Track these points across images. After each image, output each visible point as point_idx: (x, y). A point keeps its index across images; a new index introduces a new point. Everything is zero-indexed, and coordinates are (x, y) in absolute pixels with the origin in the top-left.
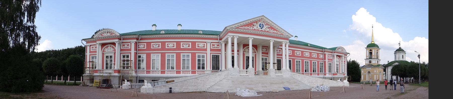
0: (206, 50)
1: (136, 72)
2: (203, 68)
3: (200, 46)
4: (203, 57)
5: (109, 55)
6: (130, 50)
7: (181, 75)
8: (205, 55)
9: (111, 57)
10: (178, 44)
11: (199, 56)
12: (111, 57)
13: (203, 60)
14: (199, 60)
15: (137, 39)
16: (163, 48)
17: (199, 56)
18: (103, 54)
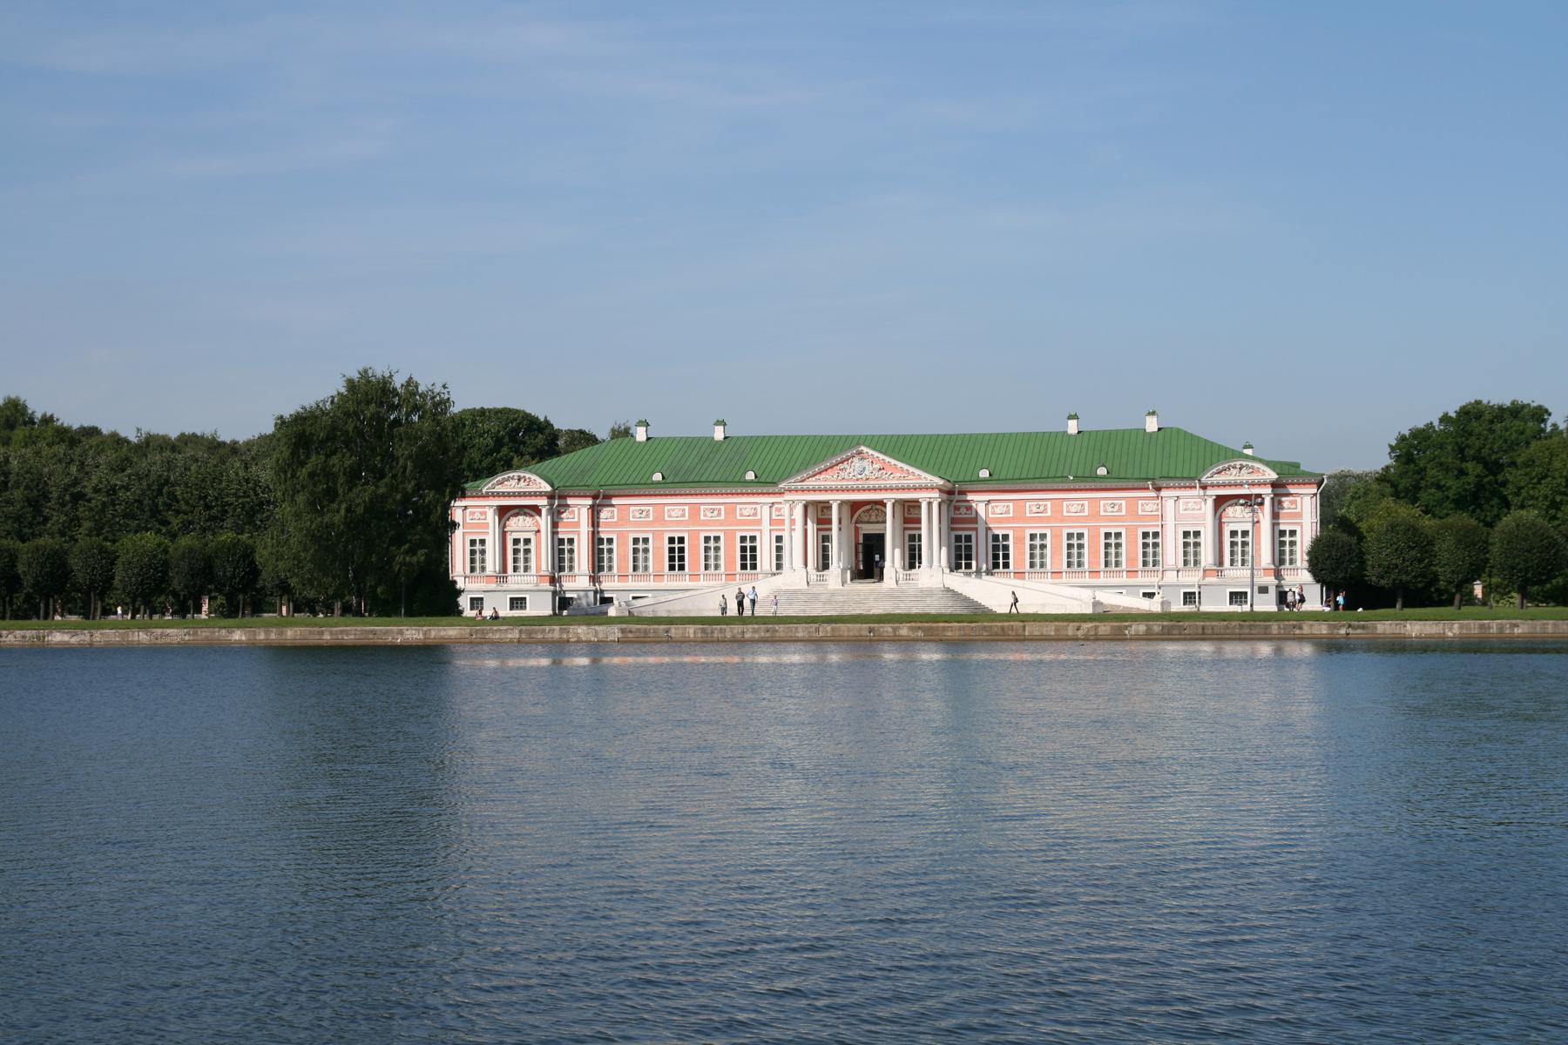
0: (759, 522)
1: (594, 579)
2: (754, 567)
3: (745, 513)
4: (753, 539)
5: (522, 536)
6: (578, 524)
7: (702, 583)
9: (527, 541)
10: (695, 510)
11: (743, 539)
12: (527, 541)
13: (753, 549)
14: (743, 549)
15: (595, 497)
16: (659, 519)
17: (743, 539)
18: (504, 535)
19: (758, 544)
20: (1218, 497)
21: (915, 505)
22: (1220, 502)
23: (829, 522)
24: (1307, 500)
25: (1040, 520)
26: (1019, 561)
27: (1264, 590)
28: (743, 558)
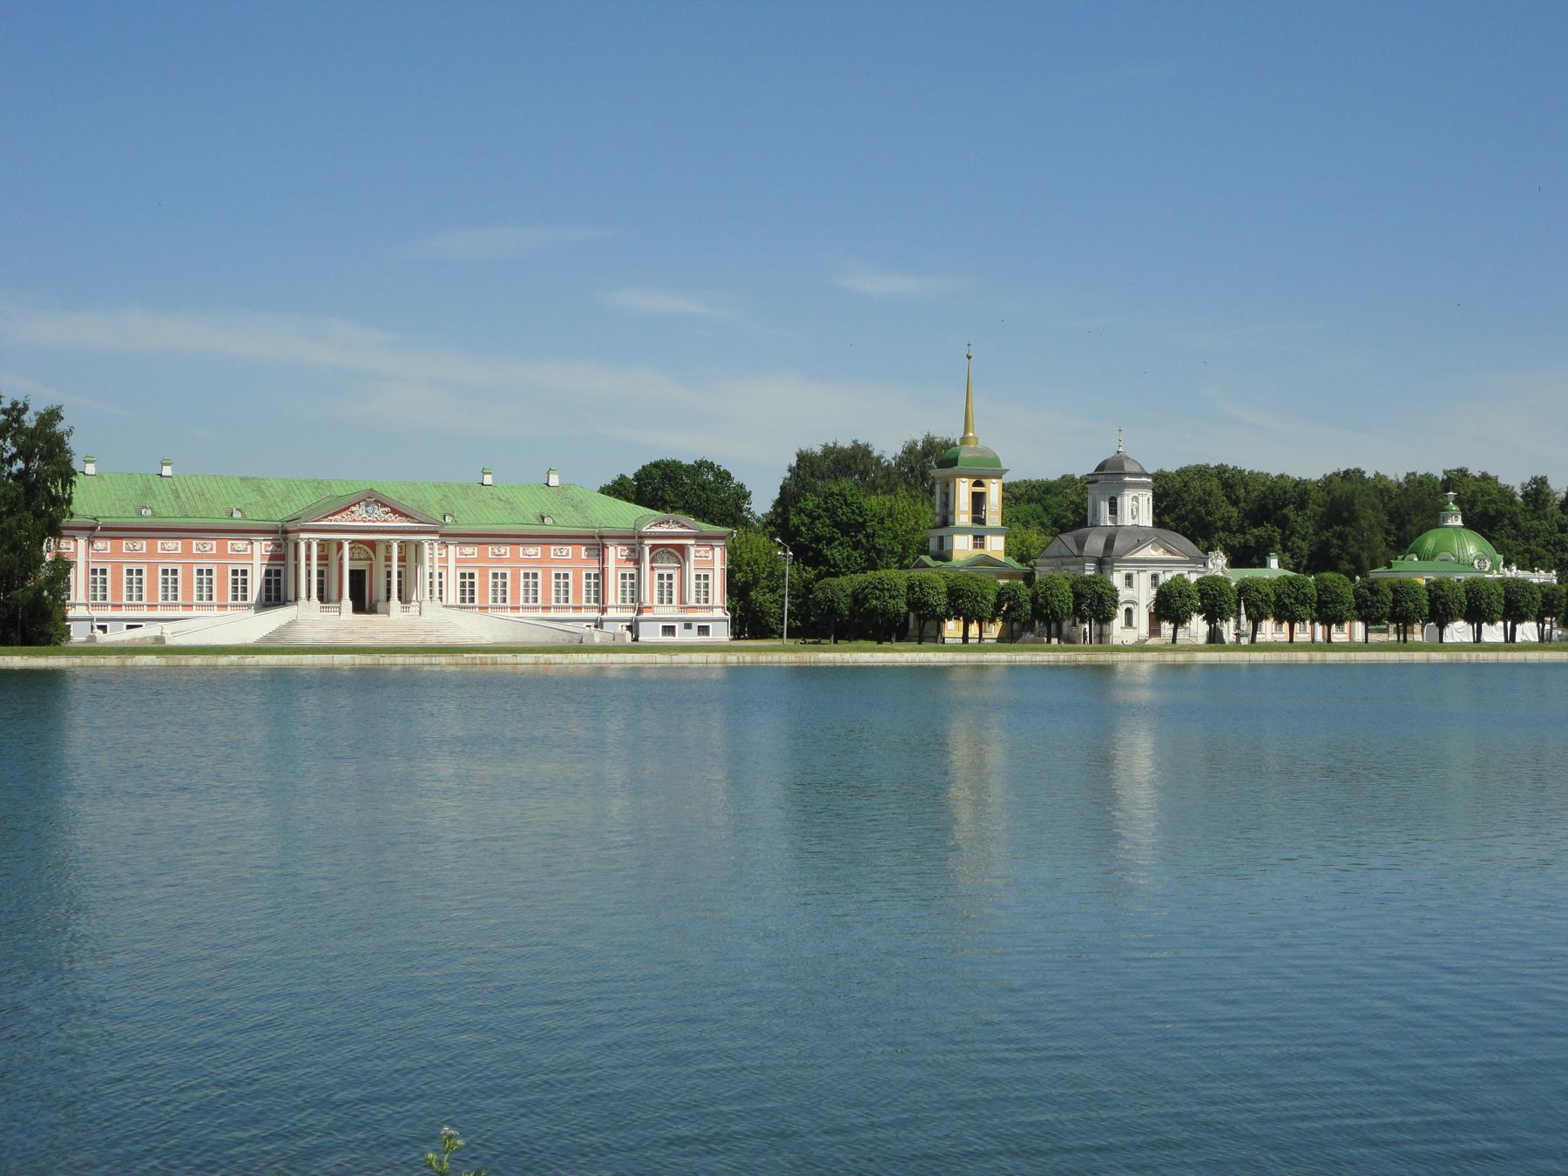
0: (251, 556)
4: (244, 572)
7: (194, 612)
8: (249, 569)
11: (235, 572)
13: (245, 581)
14: (235, 582)
19: (249, 577)
20: (653, 548)
21: (418, 546)
22: (653, 548)
23: (320, 558)
24: (717, 550)
25: (501, 560)
26: (484, 596)
27: (688, 626)
28: (235, 589)
